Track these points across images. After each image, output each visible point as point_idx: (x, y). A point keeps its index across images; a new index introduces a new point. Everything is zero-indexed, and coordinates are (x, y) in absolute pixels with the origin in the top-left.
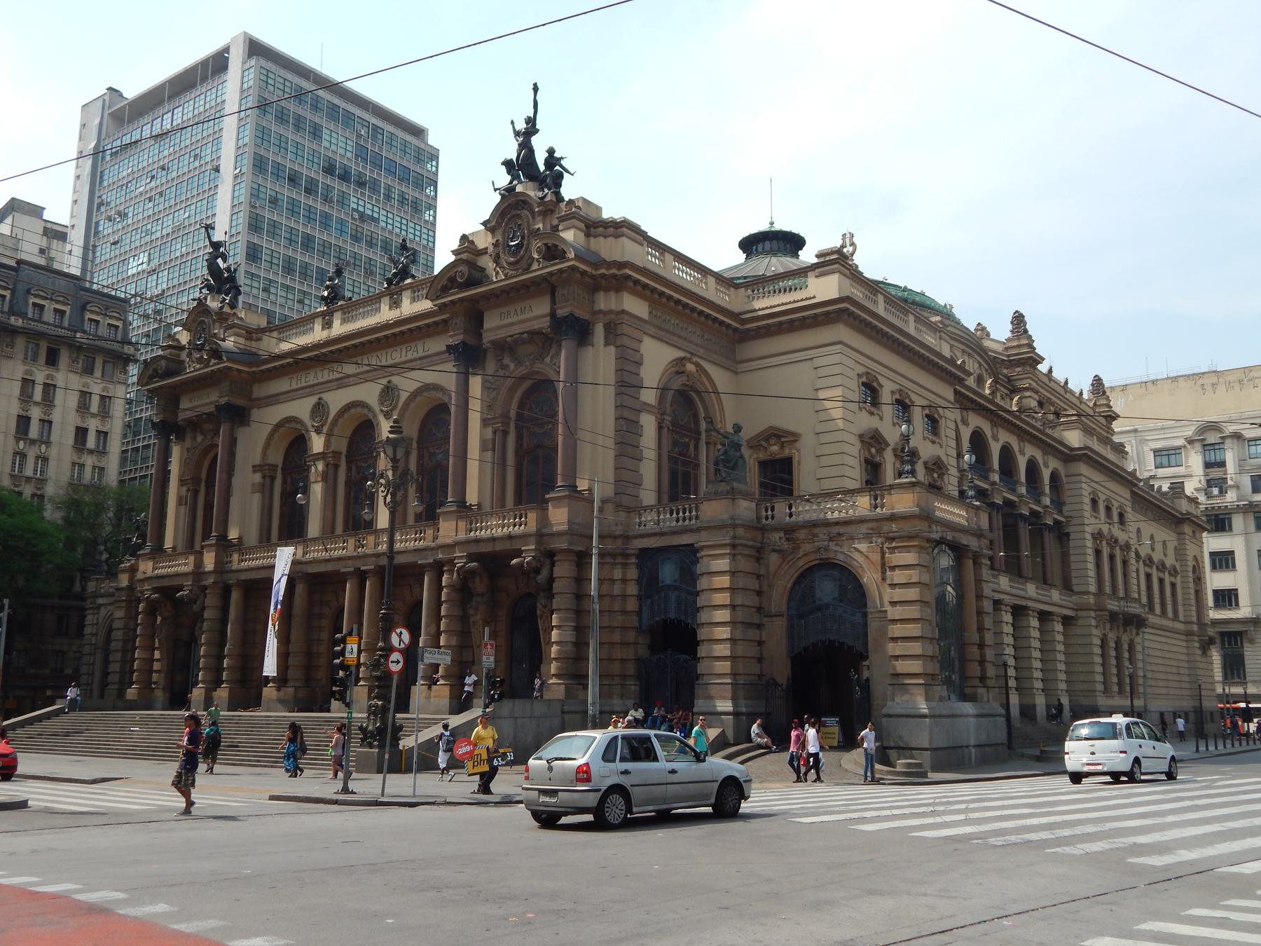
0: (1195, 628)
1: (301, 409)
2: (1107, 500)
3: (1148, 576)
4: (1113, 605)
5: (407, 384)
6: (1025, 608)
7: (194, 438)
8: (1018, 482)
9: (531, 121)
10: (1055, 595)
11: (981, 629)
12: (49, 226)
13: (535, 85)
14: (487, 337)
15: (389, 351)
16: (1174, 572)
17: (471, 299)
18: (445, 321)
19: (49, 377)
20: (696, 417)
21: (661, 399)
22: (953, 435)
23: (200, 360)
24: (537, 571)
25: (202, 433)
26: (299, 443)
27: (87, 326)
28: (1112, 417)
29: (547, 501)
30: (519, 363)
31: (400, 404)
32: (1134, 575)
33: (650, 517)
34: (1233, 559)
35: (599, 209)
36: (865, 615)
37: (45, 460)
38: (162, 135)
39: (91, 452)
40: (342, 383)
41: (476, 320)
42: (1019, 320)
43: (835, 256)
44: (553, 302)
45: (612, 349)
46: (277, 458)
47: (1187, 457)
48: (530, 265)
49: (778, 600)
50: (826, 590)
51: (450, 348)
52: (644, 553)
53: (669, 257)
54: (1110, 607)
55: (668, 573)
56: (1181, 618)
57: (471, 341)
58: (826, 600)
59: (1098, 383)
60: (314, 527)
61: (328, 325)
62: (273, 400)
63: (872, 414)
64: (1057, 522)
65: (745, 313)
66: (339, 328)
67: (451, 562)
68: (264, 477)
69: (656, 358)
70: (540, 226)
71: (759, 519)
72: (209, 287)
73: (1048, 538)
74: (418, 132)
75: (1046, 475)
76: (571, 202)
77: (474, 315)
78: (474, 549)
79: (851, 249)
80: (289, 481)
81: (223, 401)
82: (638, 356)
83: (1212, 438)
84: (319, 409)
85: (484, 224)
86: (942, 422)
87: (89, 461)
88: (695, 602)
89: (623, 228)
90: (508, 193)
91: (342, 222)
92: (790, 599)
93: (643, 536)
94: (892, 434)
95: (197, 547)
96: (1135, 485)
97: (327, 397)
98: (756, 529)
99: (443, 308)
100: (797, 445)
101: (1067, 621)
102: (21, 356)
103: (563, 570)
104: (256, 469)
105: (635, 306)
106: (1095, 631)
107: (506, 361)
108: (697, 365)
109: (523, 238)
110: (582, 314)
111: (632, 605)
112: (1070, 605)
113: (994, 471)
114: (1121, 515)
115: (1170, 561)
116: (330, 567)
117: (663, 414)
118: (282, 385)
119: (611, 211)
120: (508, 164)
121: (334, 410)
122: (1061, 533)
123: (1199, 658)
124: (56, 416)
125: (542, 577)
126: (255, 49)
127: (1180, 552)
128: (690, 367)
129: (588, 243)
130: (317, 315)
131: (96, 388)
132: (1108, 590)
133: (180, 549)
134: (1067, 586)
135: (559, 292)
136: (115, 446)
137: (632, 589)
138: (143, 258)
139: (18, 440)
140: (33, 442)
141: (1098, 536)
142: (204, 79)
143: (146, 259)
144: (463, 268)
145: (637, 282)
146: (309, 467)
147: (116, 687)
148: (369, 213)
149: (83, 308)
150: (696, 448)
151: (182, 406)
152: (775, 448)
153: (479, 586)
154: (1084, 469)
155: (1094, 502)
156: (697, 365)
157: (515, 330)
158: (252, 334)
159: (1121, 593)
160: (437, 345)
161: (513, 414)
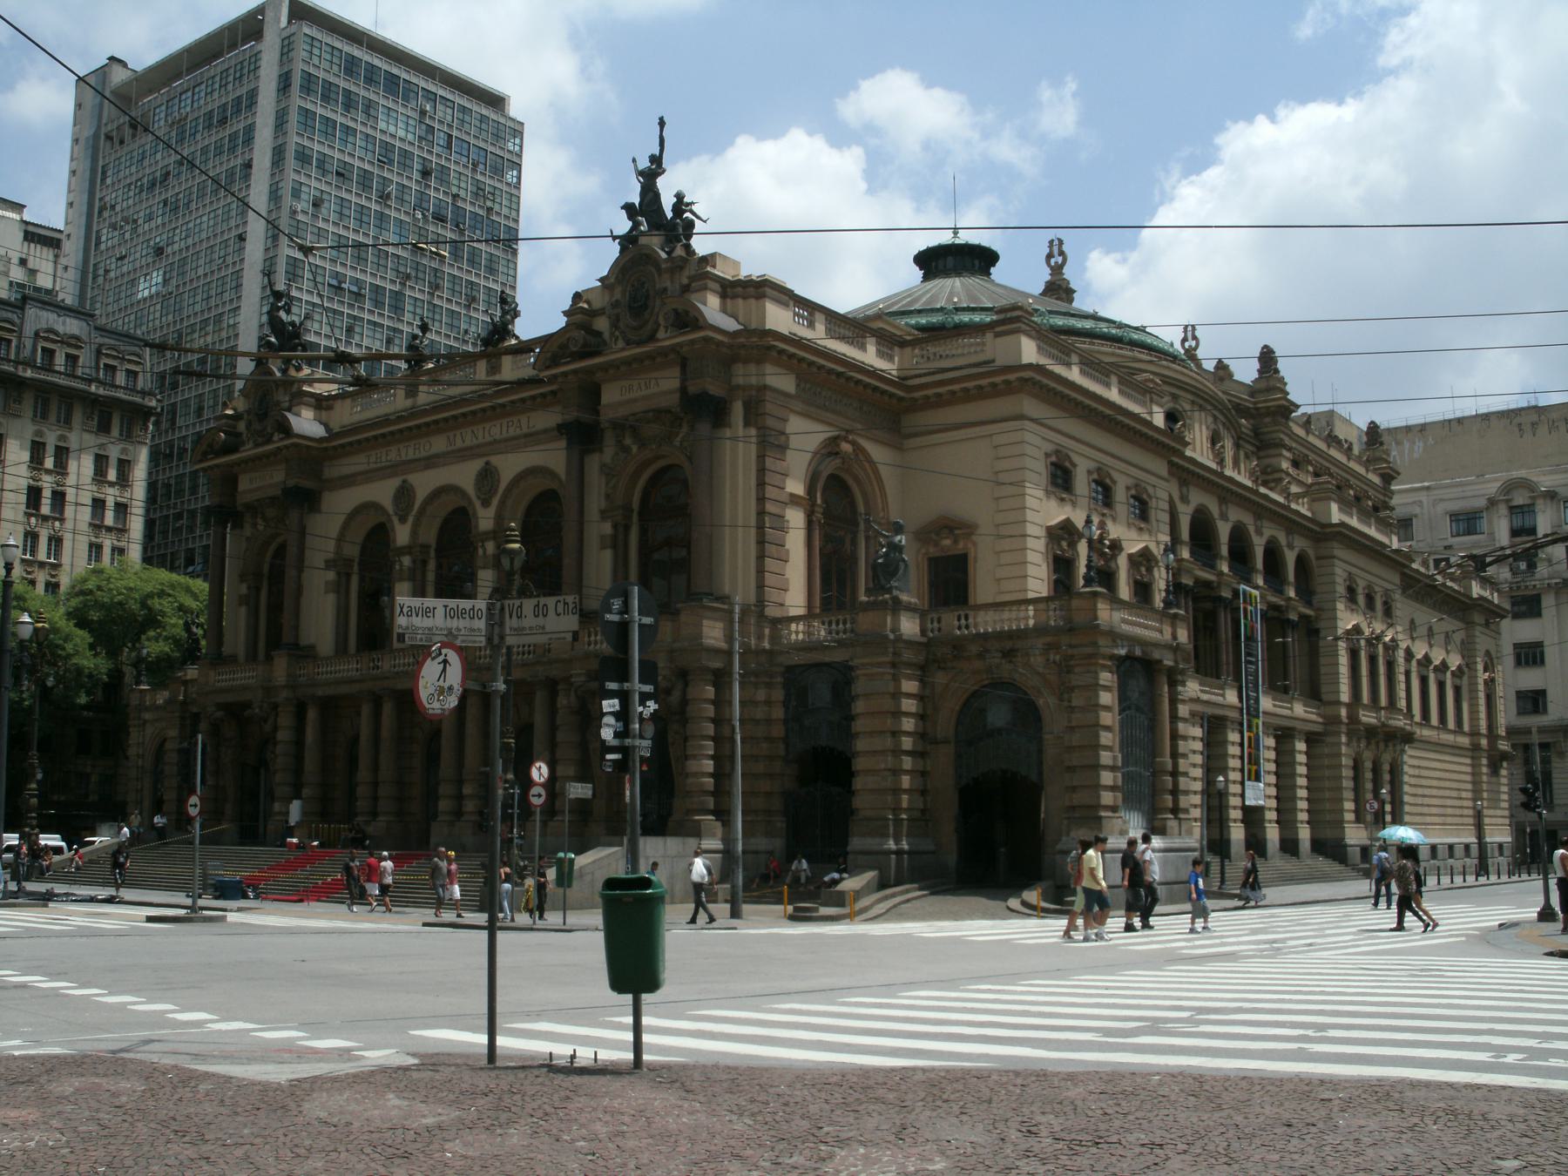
0: (1484, 742)
1: (382, 492)
2: (1369, 587)
4: (1368, 718)
5: (509, 466)
7: (255, 525)
8: (1253, 570)
9: (657, 160)
10: (1299, 709)
11: (1175, 755)
12: (31, 229)
14: (606, 415)
15: (487, 426)
17: (589, 371)
18: (553, 393)
19: (62, 438)
20: (853, 504)
21: (811, 489)
22: (1166, 517)
26: (379, 535)
28: (1388, 478)
31: (501, 491)
32: (1402, 678)
34: (1542, 654)
35: (736, 264)
40: (430, 462)
41: (592, 394)
42: (1267, 358)
43: (1015, 314)
45: (753, 432)
46: (353, 551)
47: (1490, 522)
48: (656, 331)
50: (998, 716)
51: (563, 429)
61: (412, 392)
62: (349, 481)
63: (1062, 500)
64: (1302, 617)
65: (912, 377)
68: (339, 574)
70: (668, 284)
71: (923, 632)
74: (496, 101)
75: (1290, 558)
79: (1060, 260)
81: (291, 483)
82: (783, 438)
83: (1520, 499)
84: (404, 494)
85: (601, 280)
86: (1153, 504)
89: (762, 289)
90: (627, 241)
100: (974, 538)
101: (1312, 739)
102: (30, 413)
104: (329, 564)
108: (853, 443)
110: (715, 389)
111: (778, 731)
113: (1222, 558)
119: (750, 269)
120: (629, 208)
121: (421, 495)
122: (1311, 631)
128: (846, 447)
131: (114, 452)
134: (1314, 693)
137: (778, 713)
138: (157, 277)
139: (28, 515)
140: (45, 518)
143: (160, 279)
144: (580, 335)
145: (781, 352)
150: (854, 542)
151: (241, 487)
152: (947, 542)
154: (1341, 552)
156: (853, 443)
159: (1383, 701)
160: (546, 419)
161: (636, 505)
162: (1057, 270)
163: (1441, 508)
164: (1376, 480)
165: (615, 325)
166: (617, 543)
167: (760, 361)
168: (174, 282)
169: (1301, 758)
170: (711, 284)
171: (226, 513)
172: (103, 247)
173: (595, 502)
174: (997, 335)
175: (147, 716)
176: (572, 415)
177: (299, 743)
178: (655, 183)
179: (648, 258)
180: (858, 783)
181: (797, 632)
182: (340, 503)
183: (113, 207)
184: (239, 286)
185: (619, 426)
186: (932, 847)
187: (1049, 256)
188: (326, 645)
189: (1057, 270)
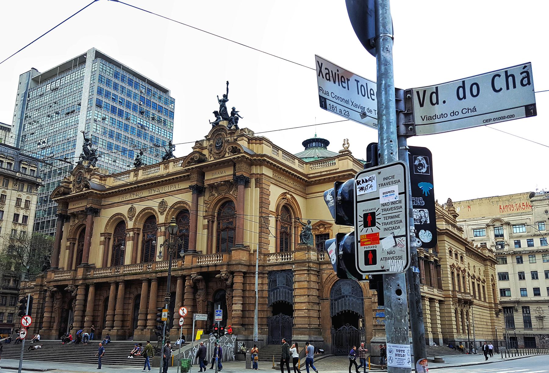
0: (493, 305)
1: (124, 210)
3: (473, 283)
4: (459, 296)
5: (171, 201)
9: (225, 96)
10: (436, 291)
13: (227, 82)
14: (206, 184)
15: (164, 187)
16: (484, 282)
18: (188, 175)
19: (3, 191)
20: (290, 216)
23: (78, 188)
24: (227, 280)
25: (78, 219)
27: (21, 170)
28: (455, 216)
29: (231, 251)
30: (219, 194)
32: (468, 283)
33: (272, 257)
34: (508, 276)
35: (253, 133)
36: (362, 300)
38: (56, 89)
39: (20, 224)
40: (142, 199)
41: (203, 175)
44: (235, 170)
48: (225, 154)
49: (327, 293)
51: (190, 187)
52: (270, 273)
53: (280, 152)
54: (458, 296)
55: (280, 281)
56: (487, 301)
57: (199, 185)
58: (346, 293)
59: (449, 200)
60: (128, 260)
64: (435, 260)
66: (141, 175)
67: (190, 276)
69: (275, 193)
70: (229, 138)
71: (318, 259)
72: (83, 158)
73: (432, 267)
74: (165, 91)
76: (242, 129)
77: (201, 173)
78: (199, 270)
79: (347, 145)
80: (116, 240)
81: (88, 206)
84: (132, 210)
85: (206, 137)
87: (19, 228)
88: (292, 293)
89: (261, 140)
90: (215, 124)
91: (133, 128)
92: (331, 293)
93: (270, 266)
95: (73, 268)
96: (467, 245)
98: (317, 263)
99: (187, 171)
100: (331, 228)
101: (441, 302)
103: (238, 279)
105: (267, 171)
106: (452, 307)
107: (214, 193)
108: (291, 195)
109: (222, 143)
112: (441, 295)
114: (461, 257)
115: (482, 278)
116: (135, 277)
117: (278, 215)
118: (116, 200)
120: (216, 113)
123: (495, 318)
125: (228, 282)
126: (98, 55)
127: (486, 272)
128: (289, 196)
129: (249, 146)
130: (132, 171)
132: (457, 289)
133: (65, 269)
134: (440, 287)
135: (237, 166)
136: (31, 222)
141: (452, 266)
142: (75, 66)
146: (126, 234)
147: (33, 329)
149: (20, 162)
150: (290, 229)
152: (322, 229)
153: (201, 285)
154: (446, 238)
155: (450, 252)
156: (291, 195)
157: (219, 180)
158: (103, 178)
159: (463, 291)
161: (216, 214)
164: (452, 217)
165: (210, 152)
166: (209, 227)
167: (260, 165)
168: (51, 142)
169: (438, 309)
170: (244, 138)
171: (64, 218)
172: (26, 130)
173: (201, 214)
175: (26, 291)
176: (194, 183)
177: (86, 300)
178: (225, 104)
179: (223, 129)
180: (296, 314)
181: (273, 259)
182: (107, 214)
183: (30, 117)
184: (74, 145)
185: (212, 186)
186: (322, 339)
187: (344, 144)
188: (99, 264)
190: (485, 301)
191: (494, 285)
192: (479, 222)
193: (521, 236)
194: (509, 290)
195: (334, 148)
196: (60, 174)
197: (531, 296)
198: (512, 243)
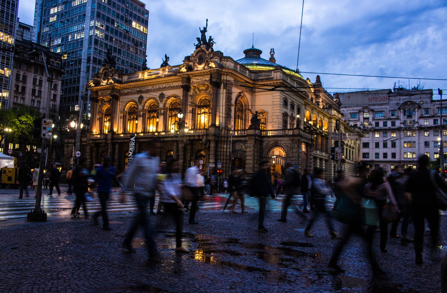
6: (317, 157)
19: (41, 78)
37: (39, 102)
51: (182, 87)
78: (188, 138)
94: (289, 113)
97: (143, 95)
101: (326, 161)
102: (33, 71)
106: (333, 164)
115: (352, 145)
120: (198, 39)
124: (43, 90)
136: (58, 99)
139: (32, 96)
140: (36, 97)
148: (128, 30)
162: (272, 56)
163: (348, 112)
169: (324, 165)
174: (274, 72)
176: (185, 84)
187: (271, 52)
189: (272, 56)
190: (352, 161)
191: (359, 150)
192: (355, 108)
193: (380, 119)
194: (368, 154)
195: (265, 56)
196: (72, 65)
197: (381, 158)
198: (374, 123)
